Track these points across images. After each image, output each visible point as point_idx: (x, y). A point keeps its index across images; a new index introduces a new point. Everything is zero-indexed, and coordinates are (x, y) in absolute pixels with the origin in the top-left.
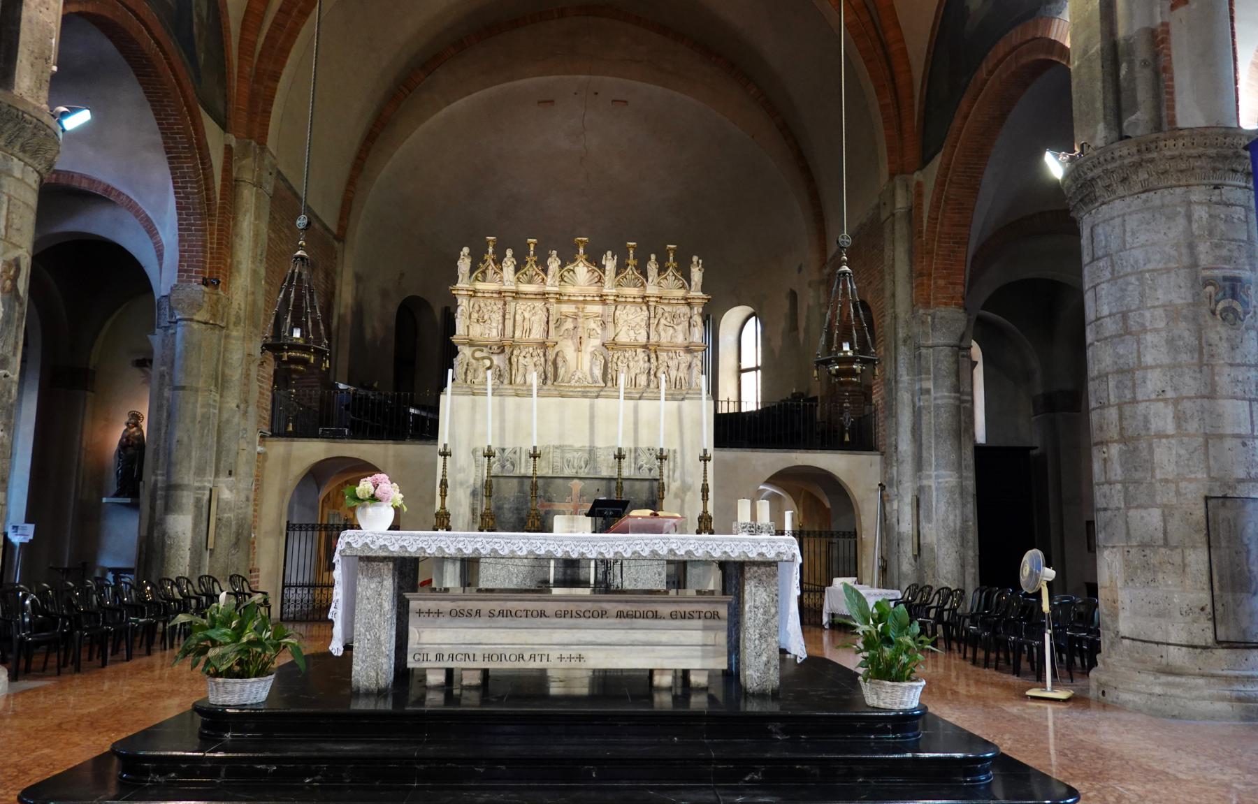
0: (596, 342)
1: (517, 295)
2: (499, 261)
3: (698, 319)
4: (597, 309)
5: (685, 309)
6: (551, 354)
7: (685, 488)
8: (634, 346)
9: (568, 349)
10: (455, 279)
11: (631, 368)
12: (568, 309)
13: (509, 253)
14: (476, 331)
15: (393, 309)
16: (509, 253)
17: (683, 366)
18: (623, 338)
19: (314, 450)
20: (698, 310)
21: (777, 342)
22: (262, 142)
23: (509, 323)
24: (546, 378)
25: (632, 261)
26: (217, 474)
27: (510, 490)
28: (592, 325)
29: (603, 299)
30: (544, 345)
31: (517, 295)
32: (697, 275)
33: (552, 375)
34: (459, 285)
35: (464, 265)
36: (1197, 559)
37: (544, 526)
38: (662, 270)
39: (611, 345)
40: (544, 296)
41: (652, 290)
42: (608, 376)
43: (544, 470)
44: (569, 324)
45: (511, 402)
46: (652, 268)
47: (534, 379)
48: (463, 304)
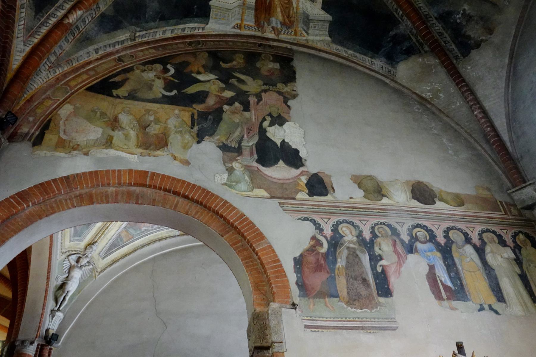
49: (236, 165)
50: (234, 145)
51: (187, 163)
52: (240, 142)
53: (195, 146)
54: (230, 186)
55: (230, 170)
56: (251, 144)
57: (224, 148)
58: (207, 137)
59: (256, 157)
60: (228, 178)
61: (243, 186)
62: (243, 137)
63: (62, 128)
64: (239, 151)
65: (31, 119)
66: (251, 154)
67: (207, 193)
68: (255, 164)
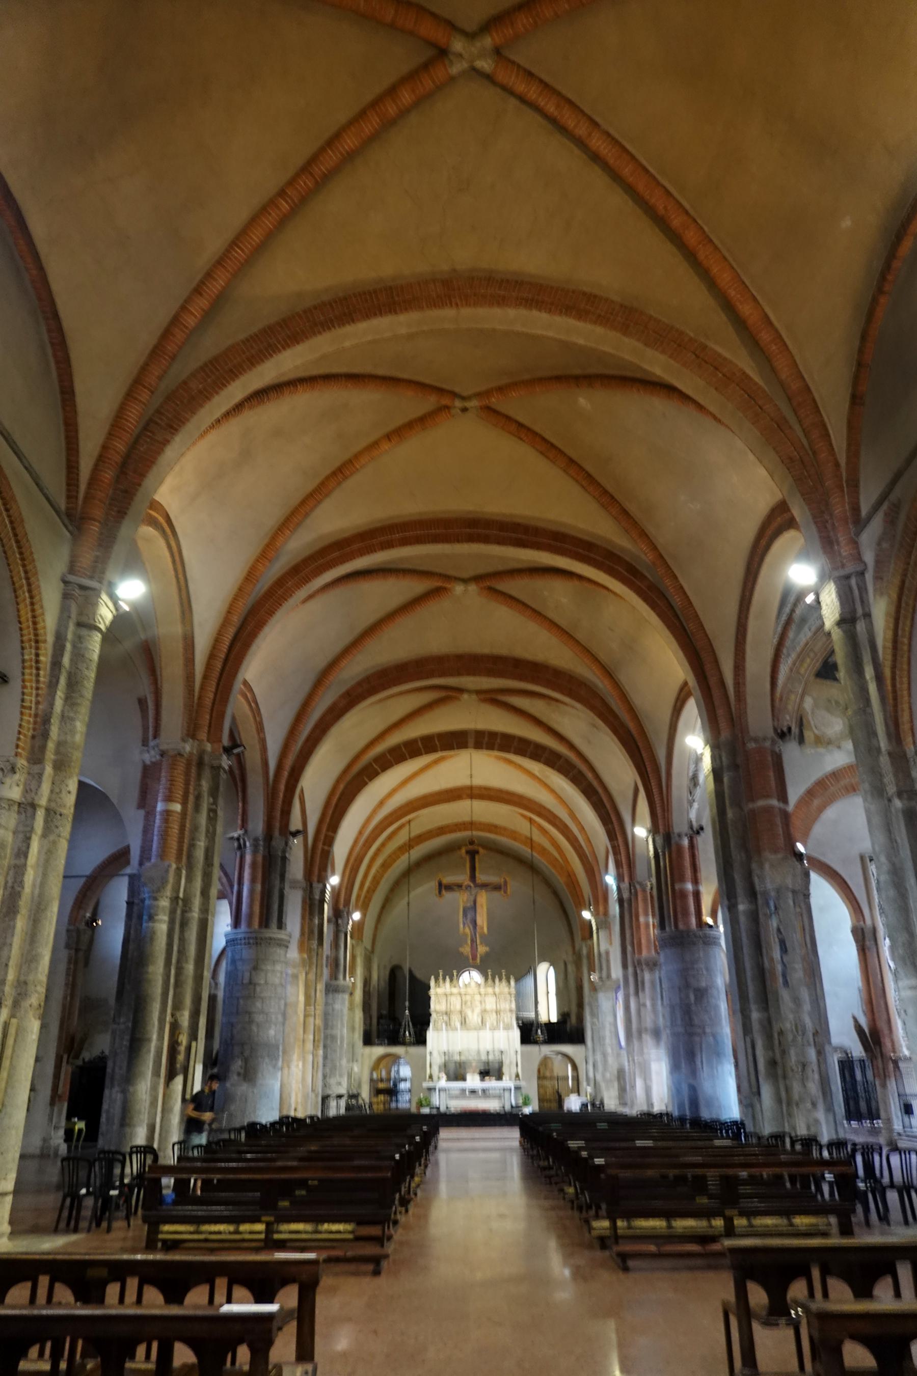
1: (451, 994)
2: (444, 979)
3: (513, 999)
7: (511, 1063)
8: (492, 1011)
9: (469, 1013)
10: (429, 988)
11: (491, 1019)
12: (468, 998)
13: (447, 977)
15: (387, 972)
16: (447, 977)
19: (379, 1051)
20: (513, 996)
21: (561, 984)
22: (362, 941)
24: (462, 1024)
25: (490, 976)
26: (353, 1061)
27: (452, 1067)
30: (461, 1012)
32: (512, 982)
33: (464, 1022)
35: (432, 983)
36: (616, 1084)
37: (464, 1079)
38: (500, 980)
39: (484, 1011)
41: (497, 990)
42: (483, 1022)
43: (463, 1058)
45: (451, 1033)
46: (497, 980)
47: (458, 1025)
63: (812, 723)
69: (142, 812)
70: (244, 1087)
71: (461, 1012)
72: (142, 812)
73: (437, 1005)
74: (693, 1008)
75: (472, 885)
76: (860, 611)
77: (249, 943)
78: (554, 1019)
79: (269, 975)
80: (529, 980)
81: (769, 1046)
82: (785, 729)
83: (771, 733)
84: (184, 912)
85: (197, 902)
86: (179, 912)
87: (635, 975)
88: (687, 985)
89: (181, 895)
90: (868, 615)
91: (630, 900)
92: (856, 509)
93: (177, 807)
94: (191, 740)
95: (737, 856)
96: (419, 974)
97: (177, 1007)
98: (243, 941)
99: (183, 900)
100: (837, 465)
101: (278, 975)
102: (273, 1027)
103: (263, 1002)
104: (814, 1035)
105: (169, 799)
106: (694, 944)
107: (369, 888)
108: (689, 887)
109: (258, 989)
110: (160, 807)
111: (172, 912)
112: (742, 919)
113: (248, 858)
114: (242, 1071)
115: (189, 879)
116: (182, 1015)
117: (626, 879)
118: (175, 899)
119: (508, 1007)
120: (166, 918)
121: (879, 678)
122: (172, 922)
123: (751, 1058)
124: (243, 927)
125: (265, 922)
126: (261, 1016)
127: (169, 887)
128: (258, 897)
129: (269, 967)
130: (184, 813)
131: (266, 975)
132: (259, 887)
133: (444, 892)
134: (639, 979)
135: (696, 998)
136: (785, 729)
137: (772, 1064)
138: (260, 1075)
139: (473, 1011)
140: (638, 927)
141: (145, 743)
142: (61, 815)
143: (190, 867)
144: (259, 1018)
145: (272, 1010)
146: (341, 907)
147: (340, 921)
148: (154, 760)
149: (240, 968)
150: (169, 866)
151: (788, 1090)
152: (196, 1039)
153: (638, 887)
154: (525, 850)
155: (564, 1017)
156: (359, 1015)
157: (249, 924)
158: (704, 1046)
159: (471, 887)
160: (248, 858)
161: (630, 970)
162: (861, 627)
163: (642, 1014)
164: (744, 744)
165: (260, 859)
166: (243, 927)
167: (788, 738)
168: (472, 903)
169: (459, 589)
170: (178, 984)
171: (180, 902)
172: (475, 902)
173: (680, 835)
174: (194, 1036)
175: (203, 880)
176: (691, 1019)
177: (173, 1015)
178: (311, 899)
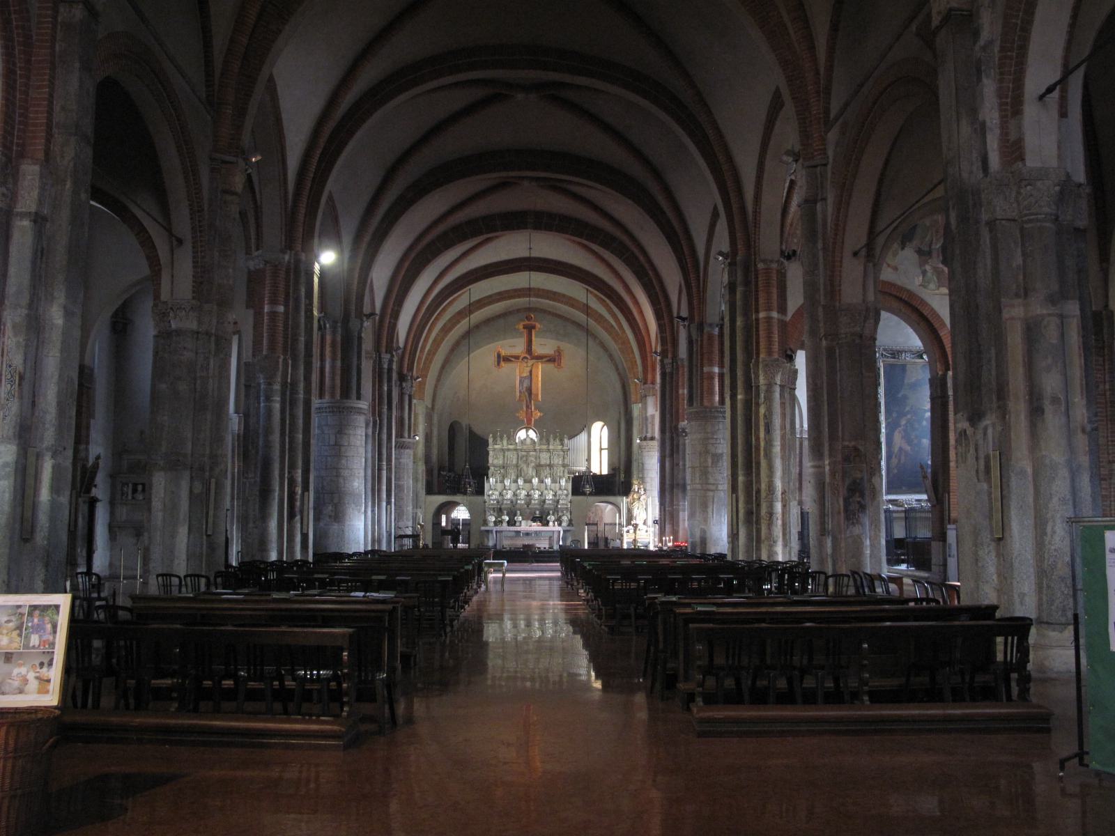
0: (533, 464)
4: (534, 453)
5: (562, 453)
6: (519, 469)
10: (488, 445)
14: (496, 462)
17: (562, 472)
18: (543, 462)
19: (441, 499)
23: (506, 459)
26: (417, 508)
28: (533, 459)
29: (535, 450)
30: (517, 466)
31: (508, 450)
34: (490, 447)
35: (491, 440)
40: (516, 450)
41: (551, 447)
44: (524, 459)
46: (552, 440)
48: (491, 453)
49: (928, 267)
50: (926, 249)
51: (896, 269)
52: (930, 247)
53: (900, 252)
54: (925, 287)
55: (924, 273)
56: (938, 246)
57: (920, 252)
58: (908, 243)
59: (941, 258)
60: (923, 280)
61: (932, 286)
62: (932, 241)
64: (929, 254)
65: (795, 240)
66: (938, 257)
67: (911, 294)
68: (941, 266)
69: (251, 312)
70: (335, 526)
71: (517, 466)
72: (251, 312)
73: (494, 460)
74: (710, 469)
75: (528, 357)
76: (819, 197)
77: (333, 412)
78: (605, 472)
79: (351, 438)
80: (583, 437)
81: (748, 500)
82: (791, 253)
83: (777, 256)
84: (292, 394)
85: (302, 385)
86: (288, 393)
87: (672, 439)
88: (707, 452)
89: (289, 381)
90: (824, 199)
91: (672, 374)
92: (827, 111)
93: (281, 309)
94: (289, 251)
95: (740, 356)
96: (478, 430)
97: (292, 467)
98: (328, 410)
99: (291, 385)
100: (818, 73)
101: (359, 437)
102: (357, 480)
103: (347, 460)
104: (782, 494)
105: (274, 302)
106: (716, 418)
107: (429, 351)
108: (716, 370)
109: (343, 449)
110: (266, 309)
111: (283, 394)
112: (740, 406)
113: (328, 338)
114: (333, 514)
115: (295, 367)
116: (297, 473)
117: (670, 356)
118: (284, 384)
119: (560, 462)
120: (278, 399)
121: (824, 249)
122: (283, 402)
123: (734, 509)
124: (327, 398)
125: (346, 394)
126: (347, 471)
127: (280, 373)
128: (339, 372)
129: (351, 432)
130: (286, 313)
131: (349, 438)
132: (339, 363)
133: (502, 363)
134: (675, 442)
135: (712, 463)
136: (791, 253)
137: (749, 513)
138: (347, 518)
139: (528, 465)
140: (677, 397)
141: (248, 252)
142: (226, 340)
143: (295, 360)
144: (345, 473)
145: (355, 467)
146: (405, 371)
147: (404, 385)
148: (258, 267)
149: (326, 432)
150: (279, 357)
151: (759, 531)
152: (308, 490)
153: (679, 363)
154: (580, 316)
155: (614, 469)
156: (422, 468)
157: (333, 395)
158: (715, 500)
159: (527, 358)
160: (328, 338)
161: (668, 434)
162: (819, 206)
163: (675, 473)
164: (756, 265)
165: (339, 338)
166: (327, 398)
167: (793, 259)
168: (528, 374)
169: (520, 96)
170: (292, 449)
171: (289, 385)
172: (531, 372)
173: (711, 325)
174: (306, 488)
175: (305, 368)
176: (707, 479)
177: (289, 473)
178: (381, 368)
